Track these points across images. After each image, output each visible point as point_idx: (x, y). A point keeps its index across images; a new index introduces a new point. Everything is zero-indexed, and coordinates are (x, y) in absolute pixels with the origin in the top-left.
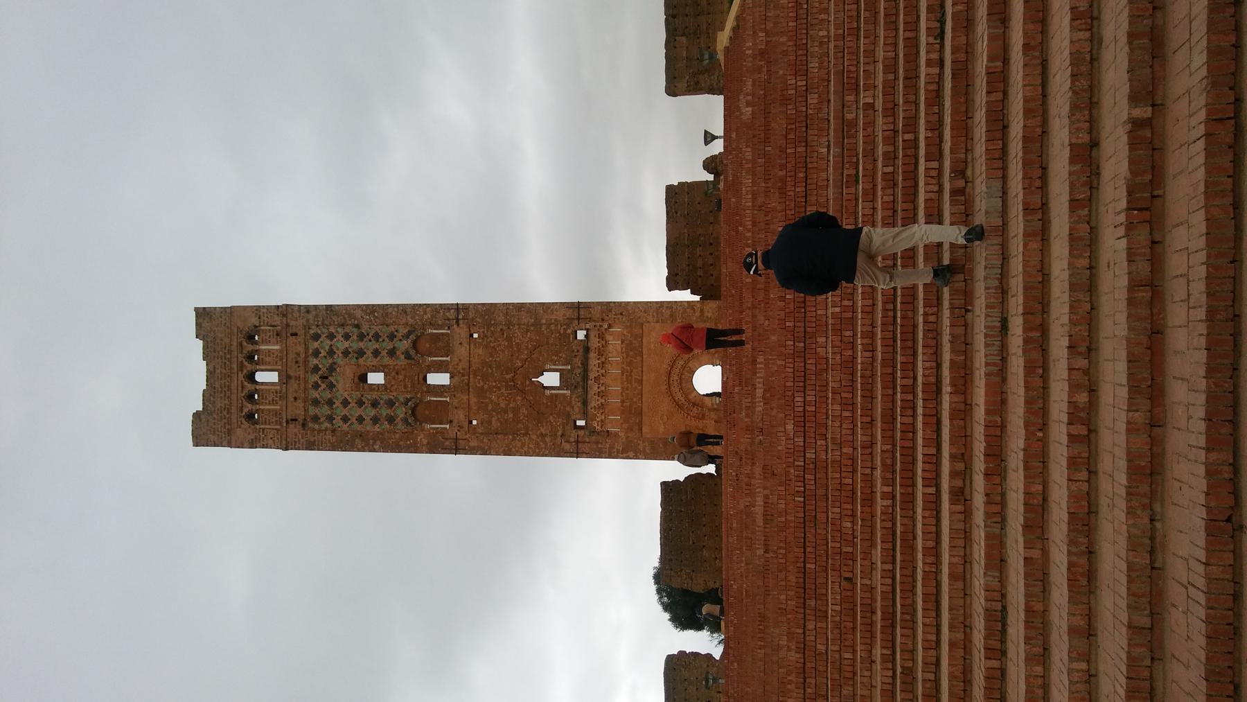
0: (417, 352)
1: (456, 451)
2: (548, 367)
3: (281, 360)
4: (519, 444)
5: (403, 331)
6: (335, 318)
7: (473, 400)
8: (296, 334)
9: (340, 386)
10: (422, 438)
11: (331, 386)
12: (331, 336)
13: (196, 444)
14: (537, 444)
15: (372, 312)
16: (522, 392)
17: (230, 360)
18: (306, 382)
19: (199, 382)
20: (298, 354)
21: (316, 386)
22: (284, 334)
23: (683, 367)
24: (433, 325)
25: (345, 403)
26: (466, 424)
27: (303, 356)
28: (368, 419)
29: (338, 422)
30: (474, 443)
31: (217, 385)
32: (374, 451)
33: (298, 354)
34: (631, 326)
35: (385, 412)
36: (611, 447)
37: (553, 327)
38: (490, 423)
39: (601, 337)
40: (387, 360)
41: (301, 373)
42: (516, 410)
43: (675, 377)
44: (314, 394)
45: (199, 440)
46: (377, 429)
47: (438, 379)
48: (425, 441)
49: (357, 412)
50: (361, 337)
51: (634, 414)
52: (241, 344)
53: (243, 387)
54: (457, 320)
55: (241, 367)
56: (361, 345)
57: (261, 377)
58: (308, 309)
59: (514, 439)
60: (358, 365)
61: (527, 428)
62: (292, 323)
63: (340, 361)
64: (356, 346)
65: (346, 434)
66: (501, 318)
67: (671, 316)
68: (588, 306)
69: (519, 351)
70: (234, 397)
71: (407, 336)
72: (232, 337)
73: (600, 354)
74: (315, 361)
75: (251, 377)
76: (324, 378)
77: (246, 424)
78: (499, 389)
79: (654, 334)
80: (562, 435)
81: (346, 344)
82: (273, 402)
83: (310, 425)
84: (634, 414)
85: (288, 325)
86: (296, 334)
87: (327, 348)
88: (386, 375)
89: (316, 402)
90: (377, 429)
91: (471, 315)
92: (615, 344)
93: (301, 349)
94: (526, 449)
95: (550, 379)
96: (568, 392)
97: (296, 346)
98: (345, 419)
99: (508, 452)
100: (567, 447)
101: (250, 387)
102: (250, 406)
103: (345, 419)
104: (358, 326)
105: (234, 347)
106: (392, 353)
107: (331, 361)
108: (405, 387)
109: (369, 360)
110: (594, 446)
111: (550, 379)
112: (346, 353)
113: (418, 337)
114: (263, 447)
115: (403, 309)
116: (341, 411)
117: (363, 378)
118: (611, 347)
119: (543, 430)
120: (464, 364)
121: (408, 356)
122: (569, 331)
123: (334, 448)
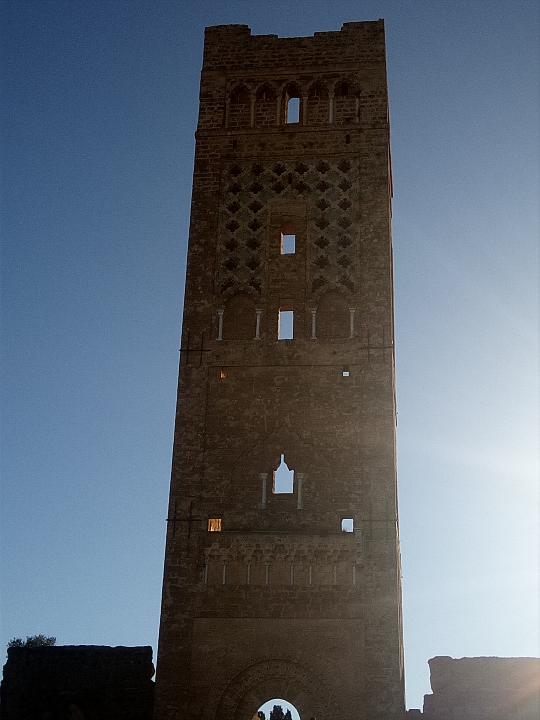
3: (315, 125)
8: (348, 141)
11: (278, 189)
12: (345, 186)
13: (208, 31)
20: (322, 145)
21: (279, 170)
22: (349, 127)
28: (233, 235)
29: (233, 198)
30: (195, 374)
32: (191, 245)
33: (322, 145)
45: (212, 34)
46: (220, 247)
48: (200, 309)
50: (345, 223)
52: (336, 76)
53: (280, 82)
55: (306, 79)
56: (334, 224)
62: (363, 137)
71: (345, 281)
74: (312, 168)
75: (294, 92)
76: (290, 178)
80: (201, 498)
81: (334, 205)
85: (360, 130)
86: (348, 141)
89: (257, 170)
90: (220, 247)
98: (234, 208)
100: (185, 506)
102: (255, 91)
103: (234, 208)
106: (322, 263)
107: (312, 186)
108: (276, 281)
123: (196, 195)
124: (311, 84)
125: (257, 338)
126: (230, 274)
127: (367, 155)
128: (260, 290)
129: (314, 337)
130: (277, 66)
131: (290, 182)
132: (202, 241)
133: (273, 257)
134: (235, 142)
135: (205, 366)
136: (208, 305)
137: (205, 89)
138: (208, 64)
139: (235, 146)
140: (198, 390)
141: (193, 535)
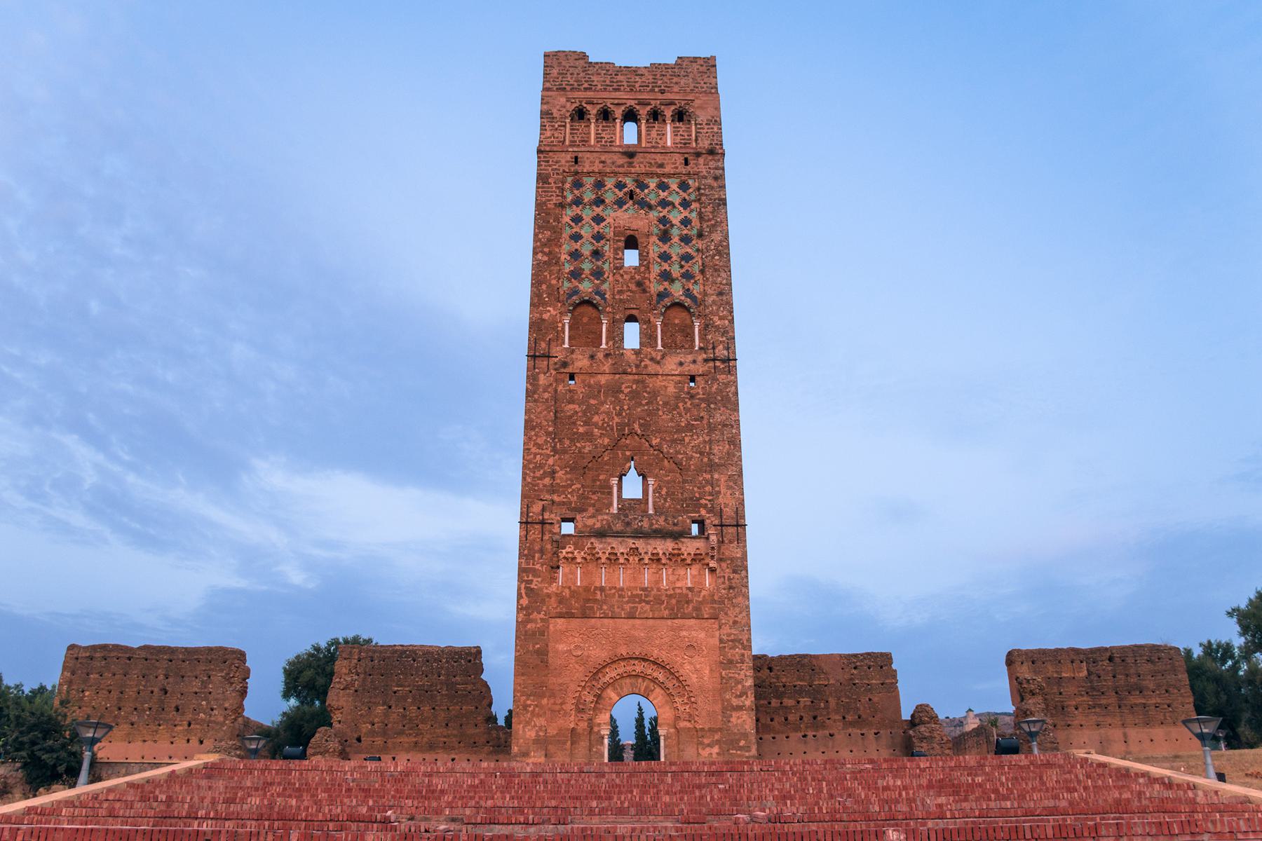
0: (668, 308)
1: (533, 357)
2: (651, 481)
4: (540, 441)
5: (696, 290)
6: (709, 209)
7: (603, 379)
8: (686, 163)
9: (619, 213)
10: (551, 312)
11: (620, 203)
12: (685, 204)
14: (541, 466)
15: (719, 253)
16: (615, 446)
17: (652, 91)
18: (626, 174)
19: (621, 60)
20: (661, 166)
21: (620, 186)
23: (654, 680)
24: (705, 328)
25: (598, 219)
26: (570, 370)
27: (659, 171)
28: (577, 246)
31: (620, 78)
32: (535, 253)
34: (714, 601)
35: (587, 266)
36: (535, 573)
37: (708, 488)
38: (571, 401)
39: (697, 558)
40: (656, 269)
41: (638, 169)
42: (588, 436)
43: (639, 667)
44: (610, 182)
45: (553, 60)
46: (564, 257)
47: (632, 335)
48: (546, 316)
49: (586, 232)
51: (583, 605)
52: (672, 103)
54: (714, 360)
55: (643, 103)
56: (676, 239)
57: (630, 128)
58: (719, 178)
59: (548, 434)
60: (648, 235)
61: (564, 452)
62: (701, 160)
63: (654, 215)
64: (675, 232)
65: (558, 220)
66: (718, 418)
67: (730, 662)
68: (740, 539)
69: (674, 441)
70: (606, 95)
71: (688, 293)
72: (678, 100)
73: (675, 557)
75: (631, 116)
76: (631, 195)
77: (571, 107)
78: (619, 414)
79: (702, 635)
80: (553, 502)
82: (599, 138)
83: (569, 179)
84: (583, 605)
85: (698, 155)
86: (686, 163)
87: (670, 199)
88: (635, 268)
89: (599, 185)
90: (564, 257)
91: (722, 378)
92: (688, 577)
93: (668, 169)
94: (534, 450)
95: (632, 487)
96: (614, 510)
97: (673, 164)
98: (577, 219)
99: (529, 426)
100: (537, 508)
101: (619, 112)
102: (595, 112)
103: (577, 219)
104: (700, 235)
105: (668, 96)
106: (666, 276)
108: (620, 292)
109: (655, 248)
110: (537, 548)
111: (632, 487)
112: (663, 220)
113: (687, 309)
114: (543, 127)
115: (724, 293)
116: (587, 214)
117: (631, 243)
118: (681, 572)
119: (560, 474)
120: (652, 368)
121: (661, 296)
122: (703, 512)
123: (540, 206)
124: (648, 108)
125: (604, 346)
126: (575, 283)
127: (706, 178)
128: (605, 299)
129: (660, 347)
130: (618, 90)
131: (631, 198)
132: (546, 250)
133: (617, 268)
134: (576, 158)
135: (554, 373)
136: (553, 313)
137: (545, 107)
138: (548, 85)
139: (576, 162)
140: (546, 395)
141: (546, 537)
